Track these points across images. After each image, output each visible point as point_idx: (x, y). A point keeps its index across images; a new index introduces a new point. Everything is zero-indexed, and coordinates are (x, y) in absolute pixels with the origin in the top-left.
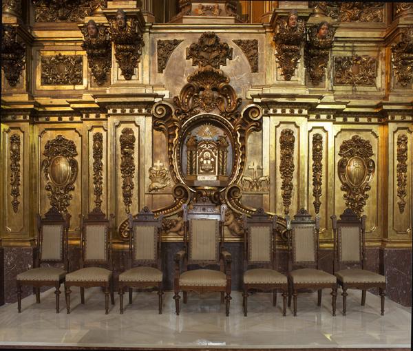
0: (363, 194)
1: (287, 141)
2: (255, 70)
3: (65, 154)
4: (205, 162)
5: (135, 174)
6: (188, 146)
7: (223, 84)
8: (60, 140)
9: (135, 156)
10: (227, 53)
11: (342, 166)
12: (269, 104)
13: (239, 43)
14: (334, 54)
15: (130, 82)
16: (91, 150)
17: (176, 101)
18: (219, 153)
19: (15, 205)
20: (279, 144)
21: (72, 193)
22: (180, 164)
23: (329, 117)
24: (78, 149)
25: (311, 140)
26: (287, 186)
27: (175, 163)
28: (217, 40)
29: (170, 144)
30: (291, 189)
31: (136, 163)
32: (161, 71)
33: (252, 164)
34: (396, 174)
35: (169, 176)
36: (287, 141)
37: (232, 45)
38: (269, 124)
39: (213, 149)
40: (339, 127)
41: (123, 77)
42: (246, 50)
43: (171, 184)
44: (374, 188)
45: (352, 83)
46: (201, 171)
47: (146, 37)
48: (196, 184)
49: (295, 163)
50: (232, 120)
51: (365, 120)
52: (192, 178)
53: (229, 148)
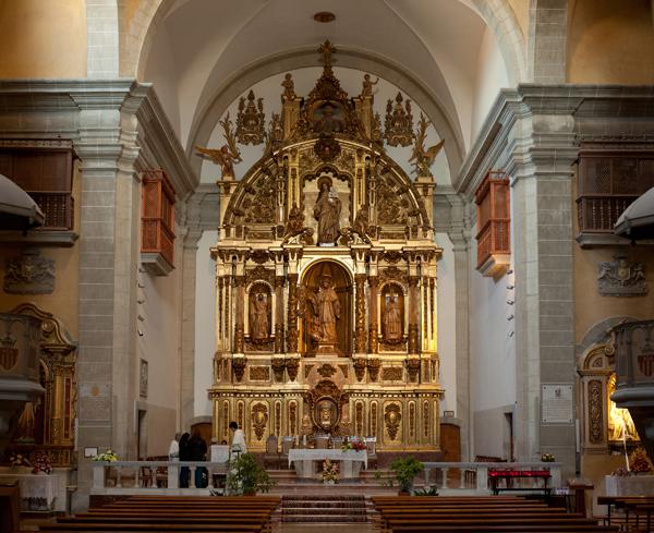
1: (359, 407)
2: (346, 377)
12: (352, 392)
26: (359, 426)
33: (345, 417)
37: (336, 367)
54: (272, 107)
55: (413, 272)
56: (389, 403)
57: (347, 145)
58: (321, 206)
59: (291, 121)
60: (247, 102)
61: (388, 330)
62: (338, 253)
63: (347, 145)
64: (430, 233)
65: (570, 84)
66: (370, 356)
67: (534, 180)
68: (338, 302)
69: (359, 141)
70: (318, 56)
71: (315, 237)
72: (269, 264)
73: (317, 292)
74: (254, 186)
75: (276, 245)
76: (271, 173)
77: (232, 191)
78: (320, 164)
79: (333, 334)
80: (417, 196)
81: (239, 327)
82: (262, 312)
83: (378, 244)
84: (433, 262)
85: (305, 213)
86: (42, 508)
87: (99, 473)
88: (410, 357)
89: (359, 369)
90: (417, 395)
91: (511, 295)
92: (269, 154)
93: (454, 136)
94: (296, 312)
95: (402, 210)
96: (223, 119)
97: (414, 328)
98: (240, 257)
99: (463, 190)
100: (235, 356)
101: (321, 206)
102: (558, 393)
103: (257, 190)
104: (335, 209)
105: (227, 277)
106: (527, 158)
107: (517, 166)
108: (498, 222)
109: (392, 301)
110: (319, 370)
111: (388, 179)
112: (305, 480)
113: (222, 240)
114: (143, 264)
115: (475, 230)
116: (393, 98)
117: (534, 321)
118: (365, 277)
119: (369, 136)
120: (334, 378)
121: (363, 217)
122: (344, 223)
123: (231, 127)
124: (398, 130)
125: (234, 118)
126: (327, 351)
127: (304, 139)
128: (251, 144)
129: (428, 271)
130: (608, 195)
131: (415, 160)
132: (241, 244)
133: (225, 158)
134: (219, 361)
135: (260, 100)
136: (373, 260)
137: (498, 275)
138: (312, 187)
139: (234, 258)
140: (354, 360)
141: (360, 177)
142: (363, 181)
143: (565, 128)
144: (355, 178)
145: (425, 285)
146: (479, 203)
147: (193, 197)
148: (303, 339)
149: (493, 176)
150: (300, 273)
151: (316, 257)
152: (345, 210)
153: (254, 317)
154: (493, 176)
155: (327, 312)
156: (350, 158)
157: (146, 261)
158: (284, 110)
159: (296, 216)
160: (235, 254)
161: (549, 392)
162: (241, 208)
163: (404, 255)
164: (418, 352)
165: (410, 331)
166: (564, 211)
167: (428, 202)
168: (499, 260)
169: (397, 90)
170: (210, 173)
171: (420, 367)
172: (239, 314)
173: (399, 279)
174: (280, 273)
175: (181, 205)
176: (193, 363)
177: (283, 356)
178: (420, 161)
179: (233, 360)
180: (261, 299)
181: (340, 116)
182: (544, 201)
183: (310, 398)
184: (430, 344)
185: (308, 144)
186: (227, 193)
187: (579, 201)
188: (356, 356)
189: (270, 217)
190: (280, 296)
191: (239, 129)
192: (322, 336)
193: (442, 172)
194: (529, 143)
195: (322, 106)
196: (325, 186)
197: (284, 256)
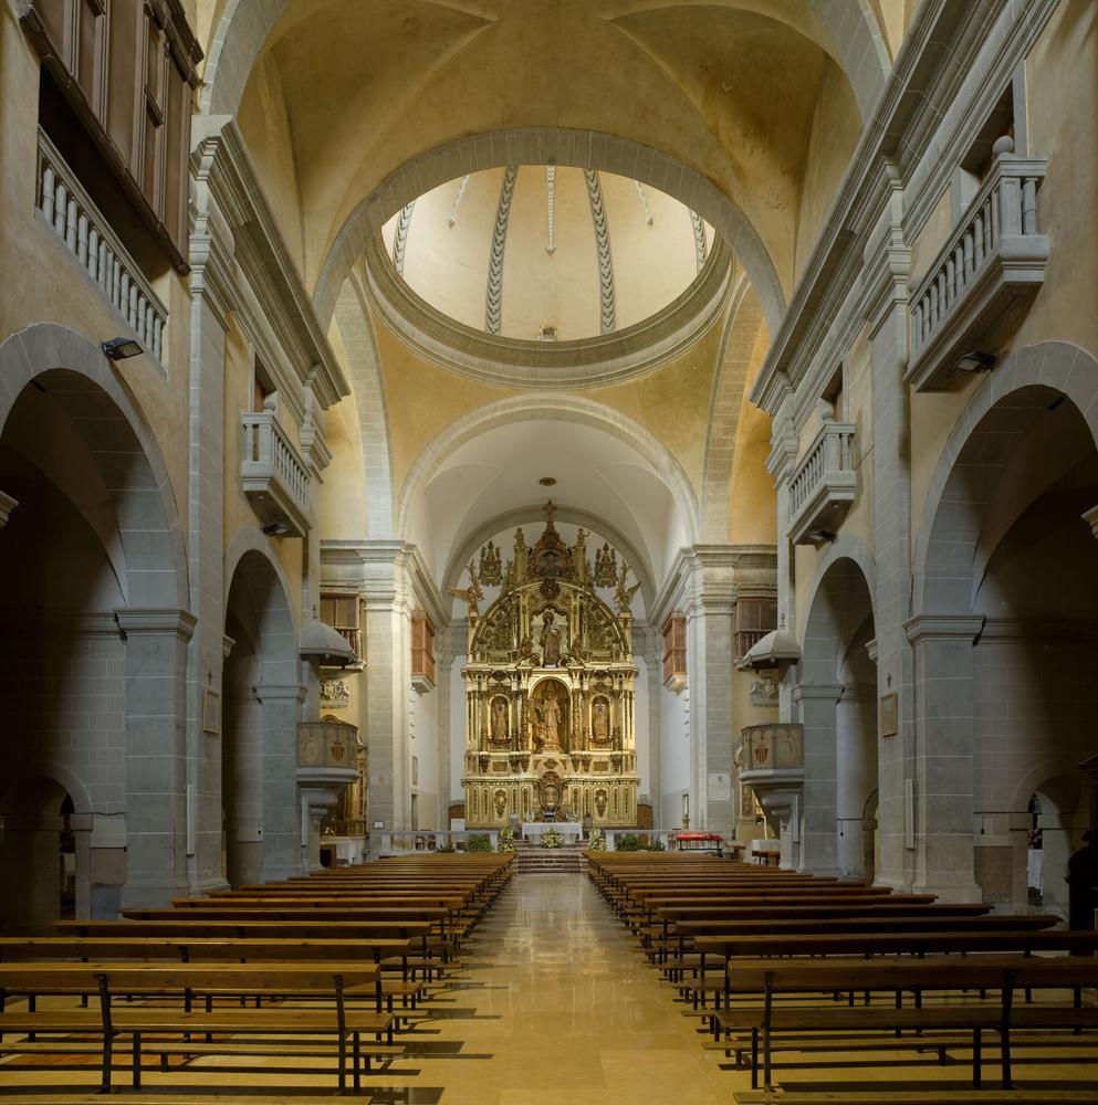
1: (576, 792)
8: (500, 791)
11: (597, 799)
12: (570, 780)
33: (565, 800)
36: (576, 792)
47: (531, 758)
54: (507, 555)
55: (616, 687)
57: (566, 587)
58: (546, 637)
59: (522, 567)
60: (487, 551)
61: (597, 732)
62: (559, 672)
63: (566, 587)
64: (629, 656)
65: (732, 543)
66: (583, 753)
67: (704, 618)
69: (574, 584)
70: (545, 512)
71: (541, 660)
72: (506, 682)
73: (543, 703)
75: (511, 667)
76: (507, 611)
77: (477, 624)
78: (543, 602)
79: (556, 735)
80: (619, 628)
81: (484, 731)
82: (502, 719)
83: (590, 666)
84: (632, 679)
85: (533, 641)
86: (346, 866)
87: (386, 840)
88: (614, 753)
89: (575, 763)
90: (620, 782)
91: (687, 706)
92: (505, 594)
93: (648, 579)
94: (527, 718)
95: (607, 639)
97: (618, 731)
99: (654, 624)
100: (482, 753)
101: (546, 637)
102: (720, 778)
103: (496, 623)
104: (557, 638)
105: (474, 692)
106: (699, 601)
107: (693, 607)
108: (677, 651)
109: (600, 710)
111: (597, 614)
112: (536, 846)
113: (471, 663)
114: (413, 684)
115: (663, 656)
116: (601, 547)
117: (703, 726)
118: (581, 691)
119: (582, 580)
121: (578, 645)
122: (563, 649)
124: (605, 574)
125: (477, 564)
127: (533, 582)
128: (491, 585)
129: (628, 686)
130: (756, 630)
131: (618, 599)
132: (485, 667)
133: (472, 597)
134: (469, 757)
135: (498, 549)
137: (679, 690)
138: (538, 621)
141: (575, 613)
142: (578, 616)
143: (727, 578)
144: (572, 616)
145: (626, 697)
146: (665, 635)
147: (448, 630)
149: (674, 615)
150: (531, 689)
151: (542, 676)
152: (564, 638)
154: (674, 615)
155: (551, 719)
156: (568, 598)
157: (415, 681)
158: (516, 558)
159: (526, 644)
160: (480, 674)
161: (714, 777)
162: (484, 638)
163: (609, 674)
164: (620, 749)
166: (725, 641)
167: (627, 633)
168: (678, 679)
169: (605, 541)
170: (460, 609)
172: (484, 721)
173: (606, 693)
174: (514, 688)
175: (438, 636)
176: (449, 760)
177: (518, 753)
178: (622, 599)
179: (480, 757)
180: (500, 709)
181: (560, 564)
182: (712, 634)
183: (538, 785)
184: (630, 743)
185: (535, 586)
186: (473, 626)
187: (736, 635)
188: (573, 752)
189: (506, 645)
190: (515, 707)
192: (547, 737)
193: (638, 608)
194: (700, 590)
195: (546, 555)
196: (548, 620)
197: (518, 675)
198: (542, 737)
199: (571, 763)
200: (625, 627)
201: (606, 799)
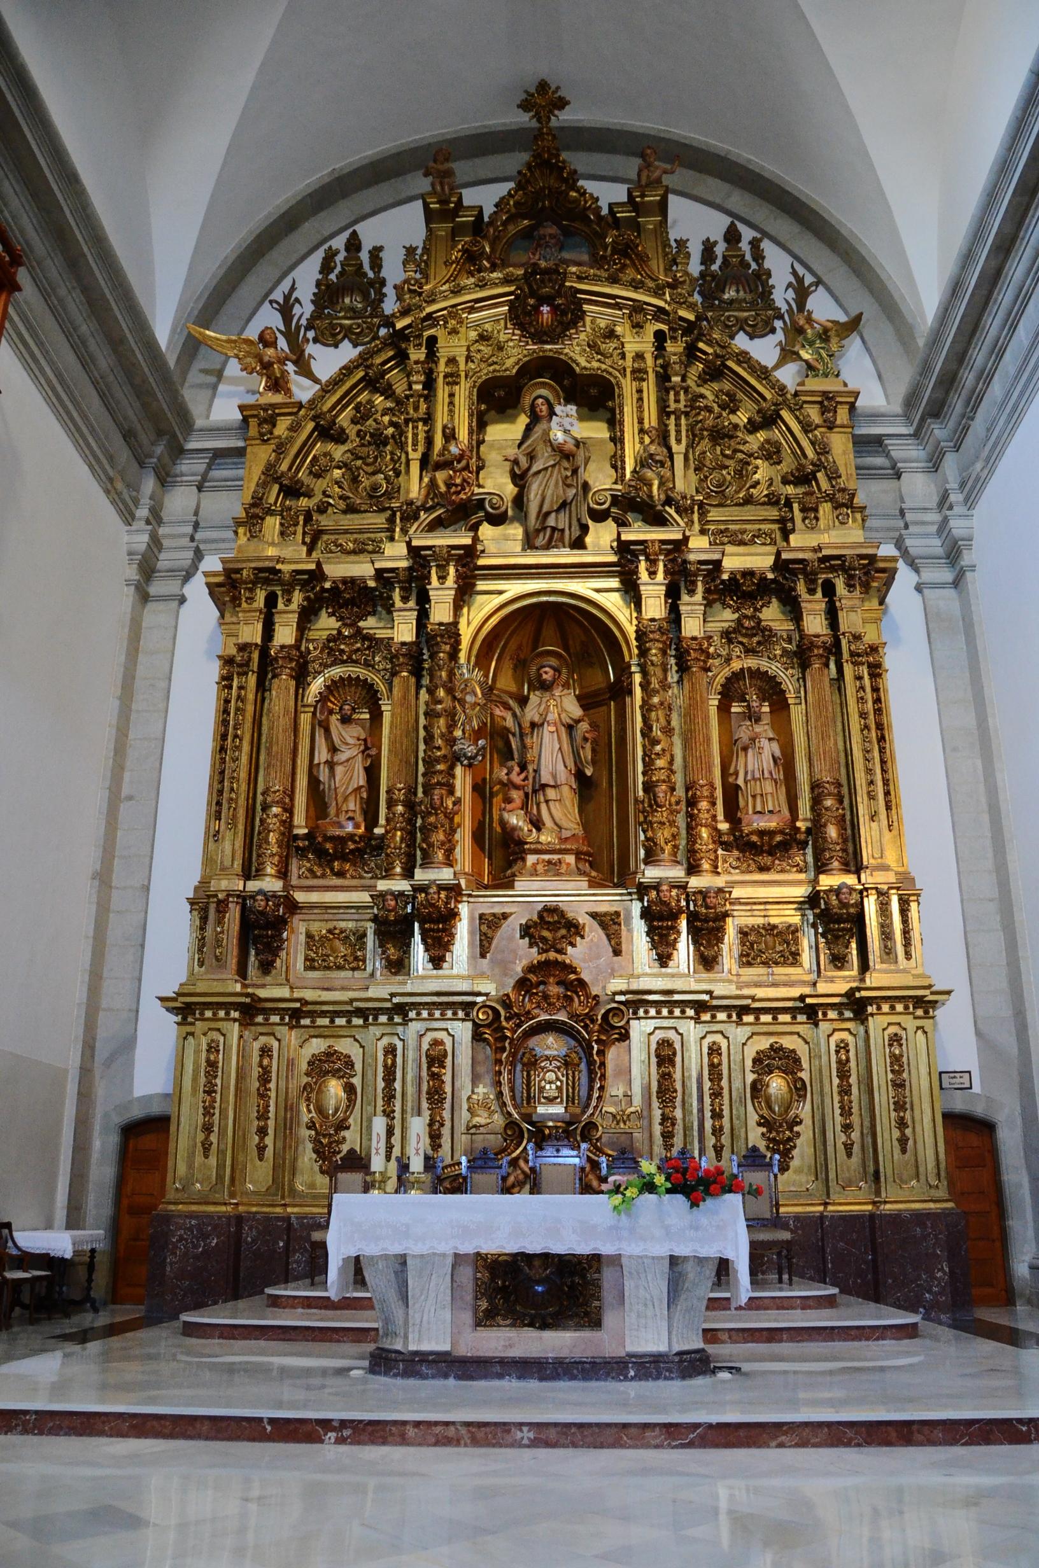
0: (791, 1131)
1: (665, 1055)
2: (617, 952)
3: (336, 1073)
4: (548, 1087)
5: (447, 1105)
6: (524, 1065)
7: (572, 977)
9: (447, 1078)
10: (574, 929)
11: (757, 1089)
12: (637, 1002)
13: (594, 915)
14: (738, 921)
15: (440, 972)
16: (380, 1069)
17: (506, 1002)
18: (567, 1074)
19: (261, 1149)
20: (654, 1060)
21: (343, 1133)
22: (512, 1090)
23: (730, 1016)
24: (358, 1067)
25: (705, 1050)
27: (506, 1090)
28: (562, 914)
29: (499, 1062)
30: (673, 1124)
31: (448, 1089)
32: (483, 956)
33: (616, 1089)
34: (836, 1098)
35: (494, 1107)
36: (665, 1055)
37: (583, 919)
38: (640, 1029)
39: (559, 1068)
40: (748, 1030)
41: (430, 966)
42: (604, 926)
43: (498, 1120)
44: (808, 1121)
45: (765, 964)
46: (543, 1100)
47: (464, 909)
48: (535, 1118)
49: (678, 1086)
50: (585, 1027)
51: (787, 1018)
52: (529, 1110)
53: (583, 1066)
56: (764, 1043)
58: (531, 457)
68: (584, 726)
74: (344, 419)
75: (395, 555)
77: (282, 427)
95: (763, 471)
96: (278, 295)
98: (288, 592)
103: (352, 431)
110: (526, 931)
120: (575, 954)
123: (297, 310)
125: (306, 292)
126: (553, 869)
136: (691, 592)
139: (271, 601)
140: (642, 890)
141: (639, 374)
142: (650, 388)
144: (628, 386)
148: (478, 836)
151: (515, 588)
153: (323, 774)
156: (610, 334)
164: (855, 865)
165: (816, 801)
167: (840, 446)
171: (859, 919)
179: (243, 898)
188: (651, 874)
191: (316, 316)
198: (516, 820)
199: (639, 927)
200: (831, 426)
201: (799, 1089)
